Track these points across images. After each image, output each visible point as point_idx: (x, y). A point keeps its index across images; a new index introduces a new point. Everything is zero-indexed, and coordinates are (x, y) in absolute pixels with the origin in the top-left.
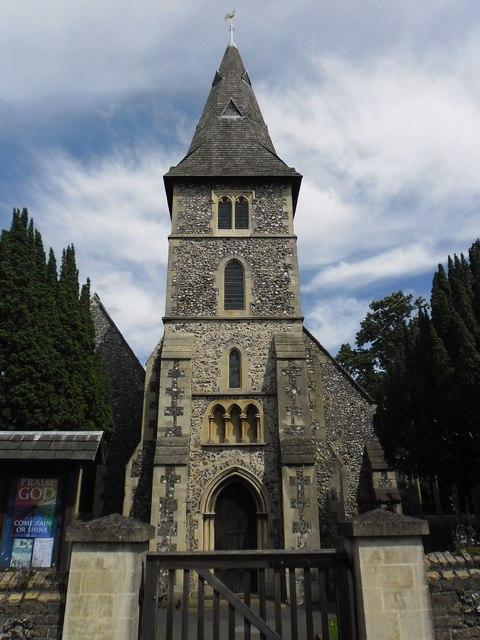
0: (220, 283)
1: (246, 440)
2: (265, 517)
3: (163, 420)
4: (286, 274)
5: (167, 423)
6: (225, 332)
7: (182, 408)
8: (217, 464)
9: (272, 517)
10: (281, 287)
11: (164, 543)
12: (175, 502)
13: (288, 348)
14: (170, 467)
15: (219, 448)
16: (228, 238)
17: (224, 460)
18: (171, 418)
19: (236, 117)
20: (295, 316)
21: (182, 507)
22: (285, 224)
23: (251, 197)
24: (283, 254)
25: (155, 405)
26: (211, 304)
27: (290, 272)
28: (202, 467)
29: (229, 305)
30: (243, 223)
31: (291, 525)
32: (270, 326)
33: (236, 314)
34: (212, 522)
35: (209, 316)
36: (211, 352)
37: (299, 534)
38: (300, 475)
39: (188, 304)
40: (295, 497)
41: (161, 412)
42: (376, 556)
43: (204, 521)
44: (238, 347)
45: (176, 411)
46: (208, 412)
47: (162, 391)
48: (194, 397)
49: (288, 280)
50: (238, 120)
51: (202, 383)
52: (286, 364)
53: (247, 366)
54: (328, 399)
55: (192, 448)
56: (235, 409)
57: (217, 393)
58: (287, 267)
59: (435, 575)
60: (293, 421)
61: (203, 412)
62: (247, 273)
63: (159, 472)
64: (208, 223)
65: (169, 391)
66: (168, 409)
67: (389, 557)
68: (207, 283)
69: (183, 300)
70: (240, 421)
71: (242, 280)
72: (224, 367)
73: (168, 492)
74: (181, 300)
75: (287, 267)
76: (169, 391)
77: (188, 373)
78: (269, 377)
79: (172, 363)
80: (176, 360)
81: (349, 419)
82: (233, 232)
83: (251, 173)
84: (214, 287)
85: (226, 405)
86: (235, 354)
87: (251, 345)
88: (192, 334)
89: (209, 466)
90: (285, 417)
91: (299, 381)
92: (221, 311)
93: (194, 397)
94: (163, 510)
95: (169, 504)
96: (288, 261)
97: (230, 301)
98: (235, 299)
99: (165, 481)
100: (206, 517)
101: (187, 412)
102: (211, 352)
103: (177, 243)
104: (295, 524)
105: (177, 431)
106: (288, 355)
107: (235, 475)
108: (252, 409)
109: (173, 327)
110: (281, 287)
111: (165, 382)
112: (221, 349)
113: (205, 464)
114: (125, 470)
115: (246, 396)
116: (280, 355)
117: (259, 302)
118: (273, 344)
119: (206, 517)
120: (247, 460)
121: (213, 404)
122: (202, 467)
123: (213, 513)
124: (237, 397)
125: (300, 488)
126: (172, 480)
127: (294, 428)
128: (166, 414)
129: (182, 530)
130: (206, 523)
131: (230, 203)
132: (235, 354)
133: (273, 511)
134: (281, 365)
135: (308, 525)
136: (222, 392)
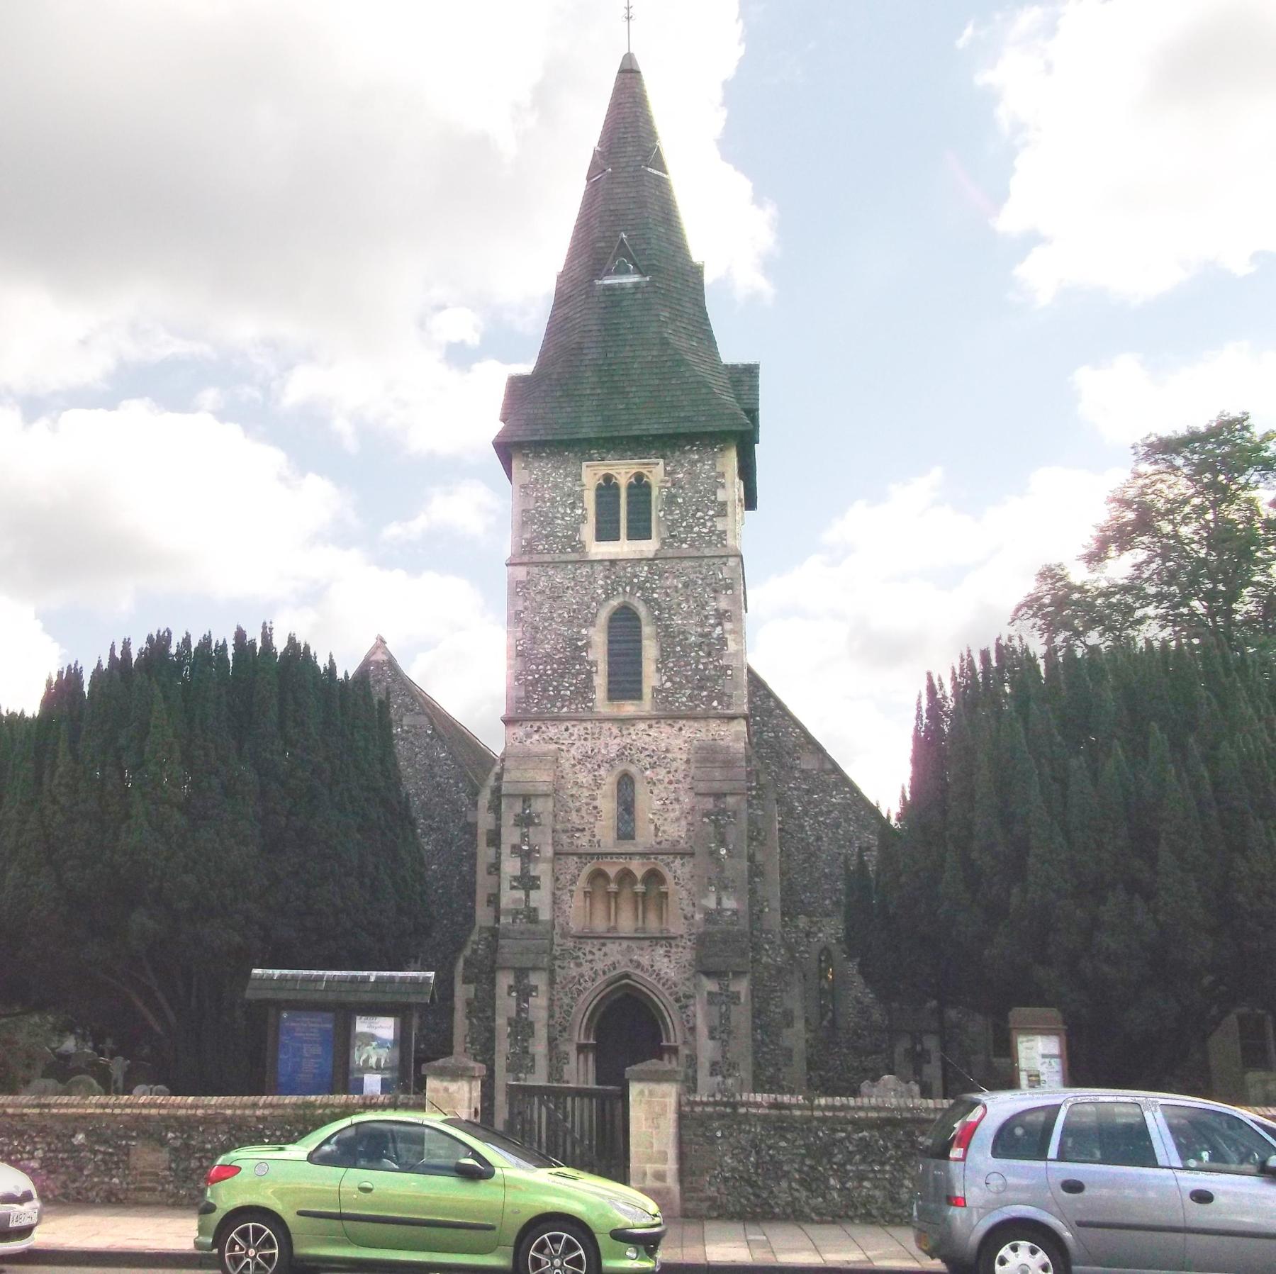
0: (598, 653)
5: (515, 901)
7: (538, 878)
12: (531, 1025)
13: (717, 774)
17: (609, 961)
18: (520, 894)
22: (720, 527)
23: (657, 472)
24: (715, 591)
25: (495, 868)
27: (728, 626)
30: (640, 530)
33: (629, 708)
36: (584, 778)
41: (505, 886)
42: (642, 1093)
44: (633, 769)
45: (527, 882)
47: (506, 850)
49: (722, 641)
53: (648, 803)
56: (626, 876)
57: (598, 850)
58: (721, 616)
59: (687, 1109)
61: (573, 882)
62: (647, 630)
63: (505, 980)
64: (577, 530)
65: (516, 849)
66: (515, 878)
67: (651, 1093)
68: (576, 650)
72: (607, 805)
73: (520, 1010)
75: (721, 616)
77: (547, 820)
78: (684, 823)
80: (526, 798)
82: (623, 548)
83: (655, 428)
84: (591, 658)
86: (626, 783)
91: (731, 835)
95: (522, 1028)
96: (723, 604)
97: (618, 683)
98: (625, 682)
99: (514, 994)
102: (584, 778)
103: (521, 573)
105: (531, 915)
107: (627, 985)
109: (520, 731)
110: (709, 654)
112: (602, 772)
113: (579, 965)
115: (643, 855)
120: (645, 961)
121: (587, 869)
124: (631, 855)
126: (524, 993)
127: (720, 912)
128: (513, 888)
129: (542, 1064)
131: (617, 487)
132: (626, 783)
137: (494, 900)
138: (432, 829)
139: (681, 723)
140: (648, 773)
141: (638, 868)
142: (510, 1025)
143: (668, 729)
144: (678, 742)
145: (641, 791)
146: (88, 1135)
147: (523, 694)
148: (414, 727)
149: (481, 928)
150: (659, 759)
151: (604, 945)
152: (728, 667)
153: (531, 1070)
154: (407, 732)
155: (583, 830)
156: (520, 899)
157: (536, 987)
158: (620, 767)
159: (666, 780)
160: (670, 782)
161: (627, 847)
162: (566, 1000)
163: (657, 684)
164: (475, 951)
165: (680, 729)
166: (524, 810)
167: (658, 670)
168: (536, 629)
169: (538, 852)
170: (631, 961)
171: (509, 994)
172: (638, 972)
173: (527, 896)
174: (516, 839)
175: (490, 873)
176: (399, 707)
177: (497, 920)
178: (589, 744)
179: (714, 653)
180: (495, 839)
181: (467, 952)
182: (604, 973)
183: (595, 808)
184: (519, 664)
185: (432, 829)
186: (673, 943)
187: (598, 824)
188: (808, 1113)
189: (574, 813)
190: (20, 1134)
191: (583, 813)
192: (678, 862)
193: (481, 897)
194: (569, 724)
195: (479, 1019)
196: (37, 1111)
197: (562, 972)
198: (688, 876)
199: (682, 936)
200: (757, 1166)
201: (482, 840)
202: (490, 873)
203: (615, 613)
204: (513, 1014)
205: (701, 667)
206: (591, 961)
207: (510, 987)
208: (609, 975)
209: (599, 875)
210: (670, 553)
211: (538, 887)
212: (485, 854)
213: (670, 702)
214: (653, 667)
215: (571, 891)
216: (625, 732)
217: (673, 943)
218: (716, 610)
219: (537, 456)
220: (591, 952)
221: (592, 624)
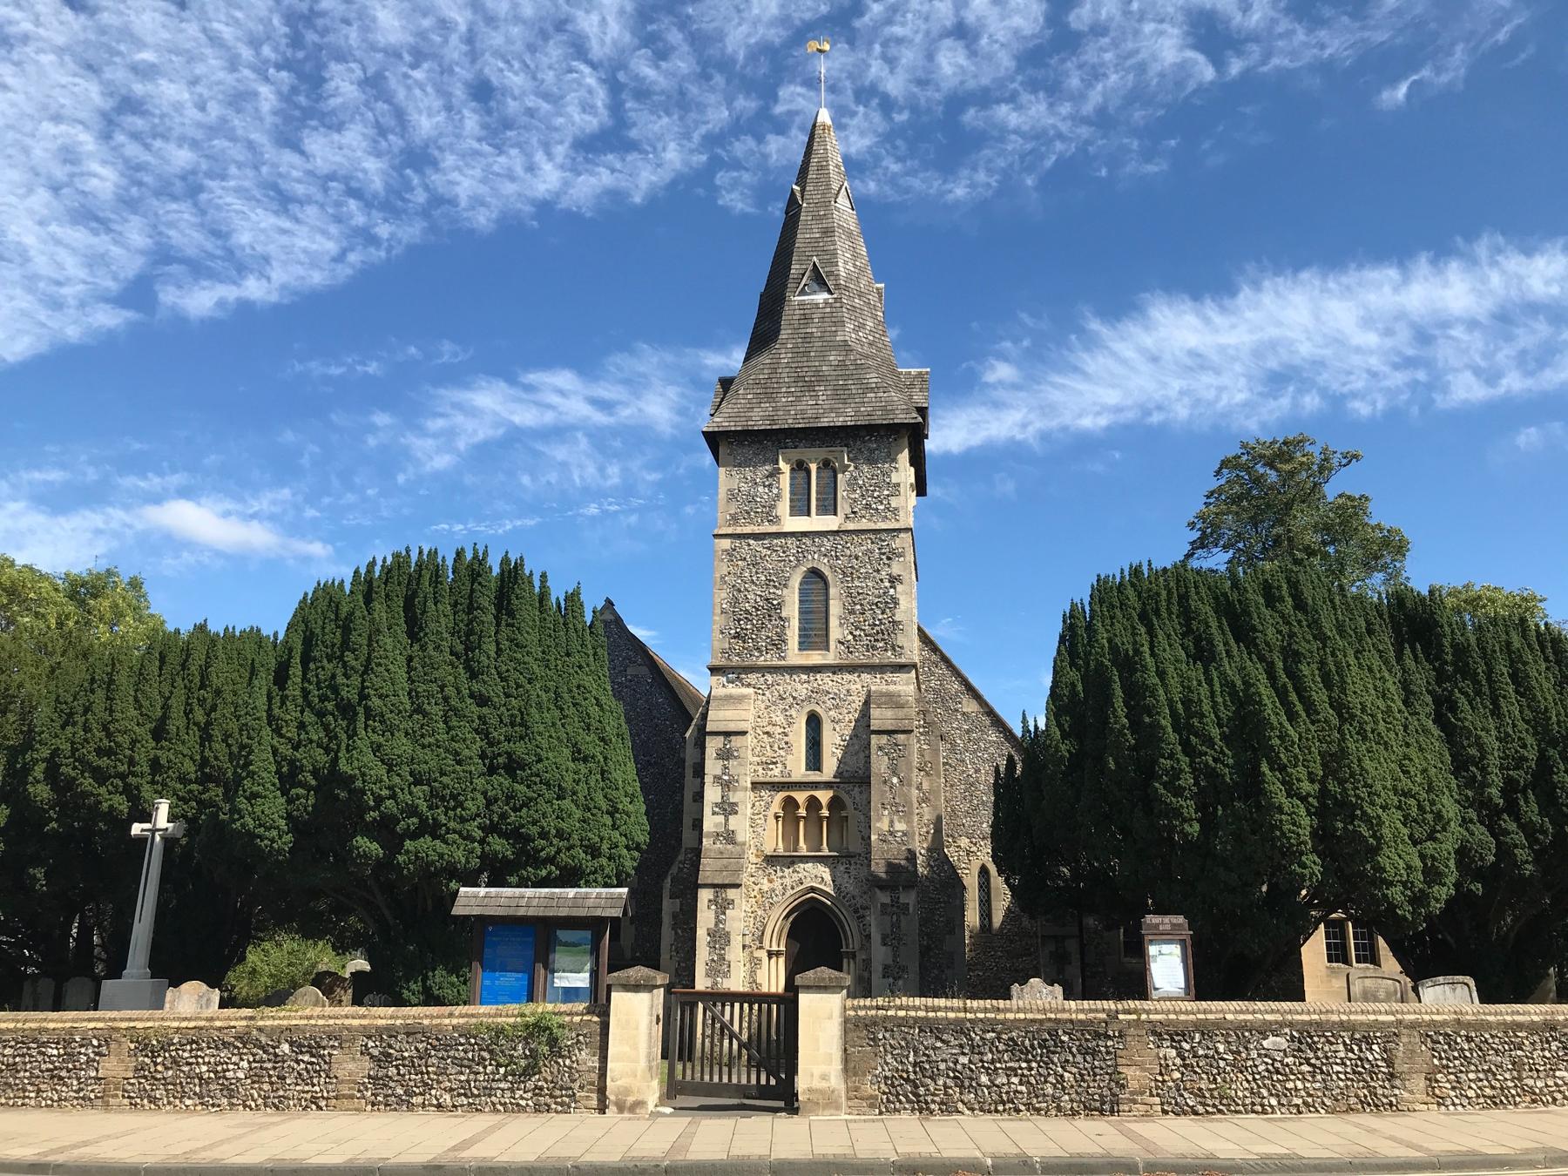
0: (792, 610)
2: (853, 956)
3: (711, 822)
4: (892, 591)
5: (716, 825)
6: (799, 686)
7: (735, 804)
8: (788, 881)
9: (861, 956)
15: (790, 861)
16: (805, 534)
17: (796, 877)
18: (721, 819)
19: (821, 297)
20: (903, 660)
21: (736, 941)
25: (699, 797)
26: (778, 643)
28: (766, 886)
29: (806, 643)
30: (828, 507)
33: (815, 658)
34: (782, 960)
35: (776, 662)
36: (779, 718)
44: (818, 709)
46: (776, 807)
47: (708, 779)
49: (896, 602)
50: (826, 302)
51: (766, 765)
52: (884, 739)
54: (977, 771)
56: (813, 803)
59: (852, 1013)
60: (892, 822)
63: (705, 895)
64: (772, 507)
66: (717, 805)
68: (773, 608)
69: (737, 636)
70: (821, 819)
75: (894, 580)
76: (717, 778)
79: (722, 738)
80: (727, 734)
84: (784, 615)
85: (801, 797)
87: (837, 707)
88: (751, 690)
89: (777, 884)
90: (879, 819)
91: (902, 763)
93: (756, 786)
95: (720, 938)
98: (815, 635)
101: (746, 810)
104: (886, 967)
105: (729, 837)
108: (835, 803)
112: (793, 712)
113: (771, 881)
118: (867, 703)
119: (770, 954)
122: (766, 886)
123: (783, 948)
124: (816, 785)
126: (722, 906)
127: (891, 833)
128: (714, 813)
130: (774, 959)
134: (874, 739)
135: (904, 969)
136: (796, 777)
137: (698, 824)
146: (291, 1044)
150: (838, 701)
153: (727, 975)
161: (814, 777)
164: (680, 870)
177: (701, 842)
180: (700, 771)
181: (674, 870)
188: (962, 1015)
190: (226, 1045)
193: (687, 821)
196: (244, 1023)
200: (915, 1064)
201: (689, 772)
204: (712, 926)
210: (851, 526)
219: (741, 444)
221: (785, 586)
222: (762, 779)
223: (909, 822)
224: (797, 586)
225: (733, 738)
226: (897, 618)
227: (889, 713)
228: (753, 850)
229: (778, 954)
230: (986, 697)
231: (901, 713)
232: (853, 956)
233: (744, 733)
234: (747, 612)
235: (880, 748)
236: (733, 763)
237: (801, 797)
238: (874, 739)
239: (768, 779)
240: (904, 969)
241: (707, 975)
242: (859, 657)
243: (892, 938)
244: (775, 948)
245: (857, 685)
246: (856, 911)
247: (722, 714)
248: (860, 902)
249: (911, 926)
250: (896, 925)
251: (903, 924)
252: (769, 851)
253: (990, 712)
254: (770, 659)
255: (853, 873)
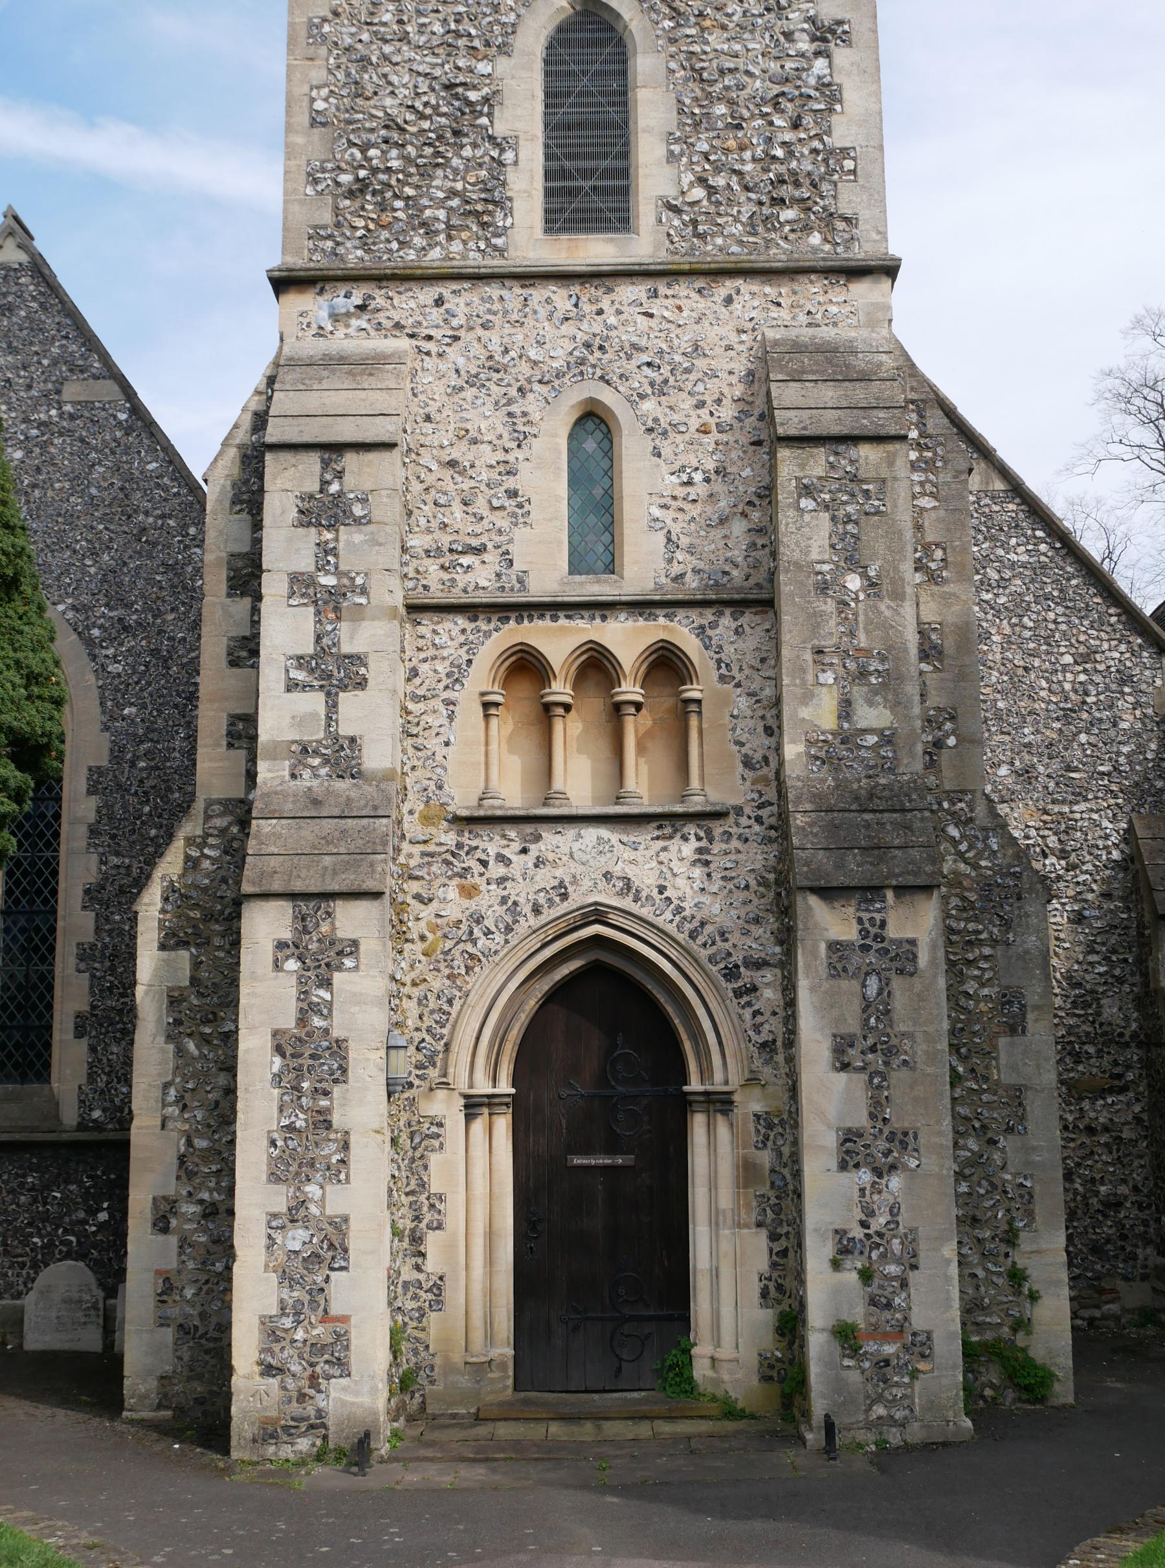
0: (522, 112)
1: (644, 786)
2: (720, 1103)
3: (283, 714)
4: (820, 65)
5: (299, 721)
6: (547, 327)
7: (358, 659)
9: (751, 1104)
10: (796, 125)
11: (296, 1213)
12: (339, 1048)
14: (312, 901)
17: (545, 878)
18: (315, 702)
21: (367, 1068)
25: (246, 651)
26: (486, 207)
28: (452, 904)
29: (568, 210)
31: (831, 1140)
32: (751, 297)
33: (596, 250)
34: (503, 1124)
35: (476, 261)
36: (486, 419)
37: (865, 1176)
38: (872, 933)
39: (383, 207)
40: (853, 1026)
43: (469, 1118)
44: (607, 396)
45: (333, 672)
46: (482, 676)
47: (273, 586)
48: (415, 609)
49: (830, 92)
52: (818, 463)
53: (645, 481)
55: (412, 827)
56: (596, 665)
60: (846, 708)
61: (456, 678)
63: (264, 927)
65: (300, 584)
66: (300, 661)
68: (465, 111)
69: (360, 189)
71: (622, 98)
72: (547, 480)
74: (351, 194)
76: (300, 584)
77: (387, 509)
78: (738, 528)
79: (313, 461)
81: (1067, 716)
84: (500, 129)
85: (558, 643)
86: (593, 420)
87: (660, 389)
88: (404, 343)
89: (488, 901)
90: (807, 697)
91: (874, 538)
92: (527, 237)
93: (415, 609)
94: (290, 1083)
95: (313, 1058)
97: (572, 193)
98: (589, 185)
99: (292, 965)
100: (472, 1106)
101: (385, 674)
104: (849, 1137)
105: (342, 756)
106: (830, 423)
107: (597, 939)
108: (666, 664)
109: (314, 306)
110: (796, 125)
111: (286, 549)
112: (532, 404)
113: (469, 892)
114: (134, 920)
115: (641, 607)
116: (789, 422)
117: (699, 193)
119: (472, 1106)
120: (646, 877)
122: (452, 904)
123: (505, 1087)
124: (602, 608)
125: (873, 984)
126: (320, 960)
128: (292, 686)
130: (478, 1126)
133: (752, 1080)
135: (903, 1140)
137: (243, 731)
138: (126, 629)
139: (728, 286)
140: (648, 406)
141: (627, 640)
142: (279, 1050)
143: (702, 304)
144: (722, 331)
145: (633, 448)
147: (327, 218)
148: (88, 404)
149: (209, 803)
151: (538, 838)
152: (845, 152)
154: (72, 417)
155: (479, 550)
156: (314, 715)
157: (355, 943)
158: (575, 395)
159: (694, 423)
160: (704, 430)
162: (437, 983)
163: (671, 192)
164: (191, 864)
165: (729, 300)
166: (325, 483)
167: (671, 157)
168: (364, 62)
169: (364, 591)
170: (607, 876)
171: (277, 966)
172: (627, 903)
173: (332, 706)
174: (305, 562)
175: (234, 663)
176: (55, 363)
178: (495, 340)
179: (808, 120)
180: (246, 577)
182: (537, 910)
183: (513, 494)
184: (313, 145)
185: (126, 629)
186: (718, 829)
187: (519, 533)
189: (457, 509)
191: (480, 506)
192: (726, 621)
193: (211, 721)
194: (445, 289)
195: (206, 1040)
197: (427, 912)
198: (751, 659)
199: (739, 811)
202: (234, 663)
203: (560, 29)
204: (288, 1021)
205: (779, 153)
206: (502, 881)
207: (281, 945)
208: (548, 914)
209: (526, 666)
211: (362, 684)
212: (220, 614)
213: (702, 236)
214: (661, 151)
215: (449, 703)
216: (587, 308)
217: (718, 831)
218: (812, 20)
220: (502, 859)
221: (504, 49)
222: (437, 595)
223: (896, 705)
224: (538, 49)
225: (350, 460)
226: (837, 140)
227: (829, 394)
228: (414, 802)
229: (490, 1102)
230: (1005, 453)
231: (860, 394)
232: (720, 1103)
233: (390, 446)
234: (390, 124)
235: (807, 490)
236: (349, 538)
237: (558, 643)
238: (788, 462)
239: (456, 596)
240: (903, 1140)
241: (275, 1178)
242: (729, 241)
243: (868, 1049)
244: (483, 1087)
245: (723, 327)
246: (731, 973)
247: (311, 402)
248: (743, 945)
249: (923, 1012)
250: (878, 1009)
251: (899, 1003)
252: (462, 801)
253: (1017, 489)
254: (462, 251)
255: (718, 862)
